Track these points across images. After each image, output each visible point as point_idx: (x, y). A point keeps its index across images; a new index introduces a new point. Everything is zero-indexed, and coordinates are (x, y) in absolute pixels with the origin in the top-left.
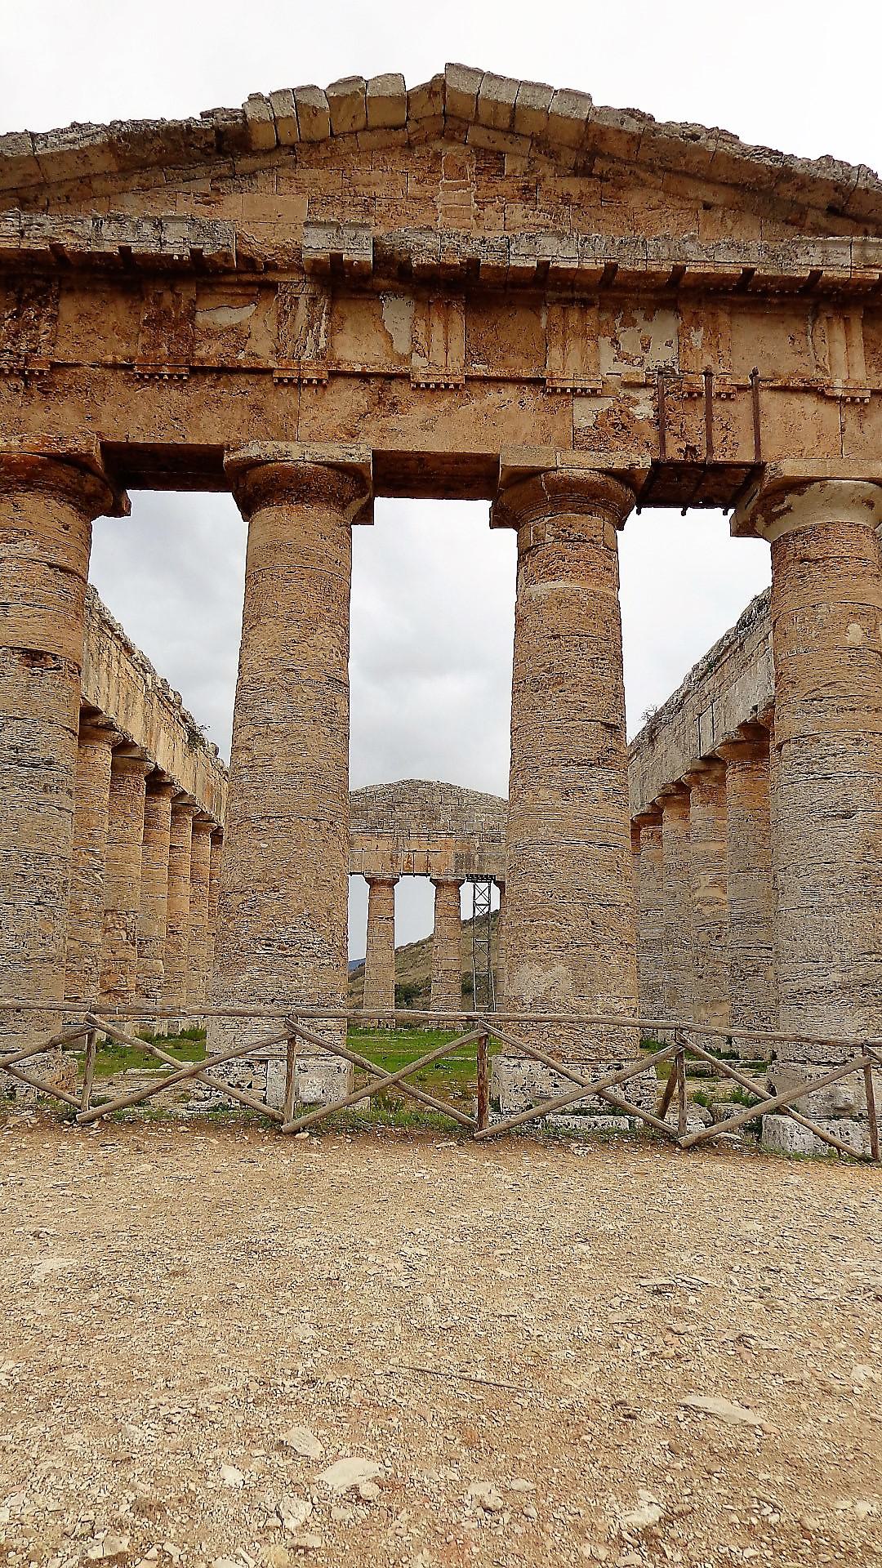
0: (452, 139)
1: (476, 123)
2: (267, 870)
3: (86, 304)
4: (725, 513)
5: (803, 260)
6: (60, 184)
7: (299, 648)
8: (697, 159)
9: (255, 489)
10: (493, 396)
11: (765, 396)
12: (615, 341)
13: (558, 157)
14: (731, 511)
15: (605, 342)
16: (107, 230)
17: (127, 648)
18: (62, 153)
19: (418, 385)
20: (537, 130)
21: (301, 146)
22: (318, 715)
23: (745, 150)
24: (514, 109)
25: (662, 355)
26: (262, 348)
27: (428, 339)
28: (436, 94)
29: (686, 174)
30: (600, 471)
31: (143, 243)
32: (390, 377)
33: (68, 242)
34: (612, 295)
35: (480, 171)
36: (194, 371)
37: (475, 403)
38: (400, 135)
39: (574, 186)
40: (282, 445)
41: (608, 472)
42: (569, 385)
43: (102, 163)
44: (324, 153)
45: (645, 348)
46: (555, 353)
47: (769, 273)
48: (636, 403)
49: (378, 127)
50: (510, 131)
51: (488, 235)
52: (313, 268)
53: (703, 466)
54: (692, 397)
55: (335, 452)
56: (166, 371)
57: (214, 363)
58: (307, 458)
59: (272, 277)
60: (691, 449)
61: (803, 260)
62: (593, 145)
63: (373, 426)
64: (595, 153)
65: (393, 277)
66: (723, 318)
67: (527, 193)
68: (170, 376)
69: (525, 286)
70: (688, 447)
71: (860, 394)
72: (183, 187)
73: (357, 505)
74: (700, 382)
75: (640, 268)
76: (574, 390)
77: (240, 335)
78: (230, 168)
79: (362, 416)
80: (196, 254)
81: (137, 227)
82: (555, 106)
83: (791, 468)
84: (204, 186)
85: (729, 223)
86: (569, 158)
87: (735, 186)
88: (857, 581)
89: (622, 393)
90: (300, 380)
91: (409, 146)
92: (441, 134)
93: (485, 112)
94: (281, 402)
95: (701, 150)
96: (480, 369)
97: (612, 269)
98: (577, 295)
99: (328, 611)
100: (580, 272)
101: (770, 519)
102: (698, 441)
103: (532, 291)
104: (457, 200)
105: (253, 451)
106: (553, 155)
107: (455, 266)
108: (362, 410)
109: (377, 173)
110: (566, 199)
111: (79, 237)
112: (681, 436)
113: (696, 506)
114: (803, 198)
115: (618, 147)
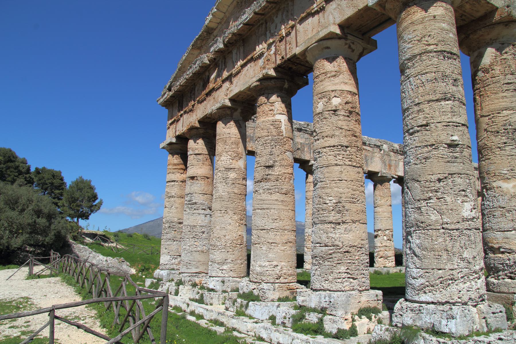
22: (222, 180)
71: (321, 5)
88: (322, 83)
99: (225, 149)
102: (284, 53)
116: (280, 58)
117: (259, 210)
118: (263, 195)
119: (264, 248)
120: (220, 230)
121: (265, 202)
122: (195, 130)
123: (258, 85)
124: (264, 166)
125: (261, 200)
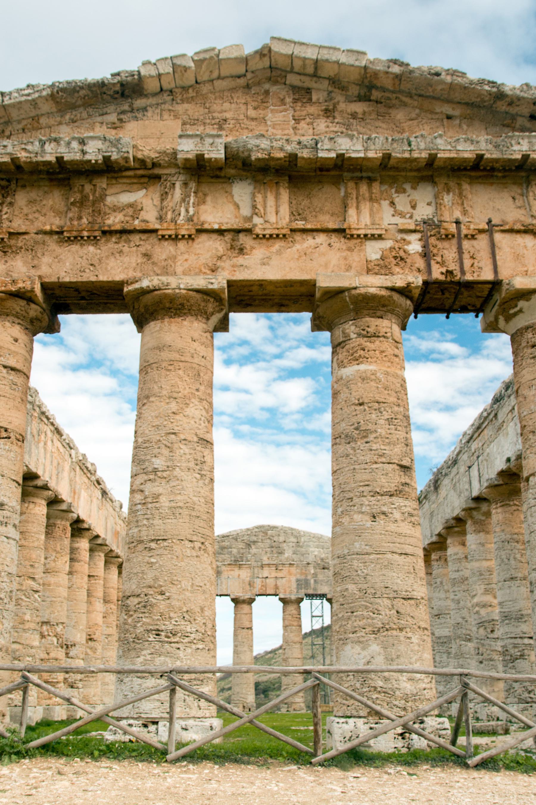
0: (276, 83)
1: (292, 71)
2: (156, 579)
3: (33, 194)
4: (477, 316)
5: (516, 148)
6: (19, 122)
7: (177, 417)
8: (440, 87)
9: (147, 309)
10: (310, 241)
11: (498, 237)
12: (392, 204)
13: (347, 90)
14: (481, 315)
15: (385, 204)
16: (48, 147)
17: (58, 432)
18: (20, 102)
19: (258, 236)
20: (332, 74)
21: (176, 90)
22: (192, 465)
23: (471, 82)
24: (316, 61)
25: (424, 211)
26: (150, 216)
27: (265, 207)
28: (264, 55)
29: (434, 98)
30: (387, 288)
31: (71, 154)
32: (238, 231)
33: (23, 155)
34: (388, 173)
35: (295, 101)
36: (104, 233)
37: (298, 246)
38: (242, 81)
39: (359, 108)
40: (164, 279)
41: (393, 289)
42: (362, 232)
43: (46, 107)
44: (191, 93)
45: (414, 207)
46: (352, 212)
47: (494, 156)
48: (409, 243)
49: (227, 77)
50: (315, 75)
51: (302, 139)
52: (185, 164)
53: (459, 283)
54: (448, 237)
55: (200, 282)
56: (85, 234)
57: (118, 227)
58: (182, 286)
59: (157, 171)
60: (449, 273)
61: (516, 148)
62: (370, 82)
63: (226, 264)
64: (371, 87)
65: (240, 167)
66: (466, 186)
67: (329, 113)
68: (88, 237)
69: (328, 170)
70: (447, 271)
72: (99, 119)
73: (215, 319)
74: (453, 228)
75: (407, 155)
76: (366, 235)
77: (135, 209)
78: (130, 106)
79: (220, 258)
80: (107, 159)
81: (69, 143)
82: (343, 59)
83: (520, 283)
84: (113, 118)
85: (465, 127)
86: (354, 90)
87: (467, 104)
89: (399, 236)
90: (177, 236)
91: (248, 87)
92: (269, 79)
93: (297, 65)
94: (163, 251)
95: (443, 82)
96: (300, 224)
97: (387, 157)
98: (364, 174)
99: (198, 390)
100: (365, 159)
101: (508, 318)
102: (453, 267)
103: (332, 173)
104: (281, 119)
105: (145, 283)
106: (343, 88)
107: (280, 159)
108: (219, 254)
109: (227, 105)
110: (354, 115)
111: (30, 152)
112: (442, 264)
113: (455, 311)
114: (513, 110)
115: (388, 83)
116: (444, 270)
117: (396, 556)
118: (402, 524)
119: (415, 640)
120: (192, 592)
121: (408, 540)
122: (23, 303)
123: (383, 297)
124: (398, 465)
125: (400, 534)
